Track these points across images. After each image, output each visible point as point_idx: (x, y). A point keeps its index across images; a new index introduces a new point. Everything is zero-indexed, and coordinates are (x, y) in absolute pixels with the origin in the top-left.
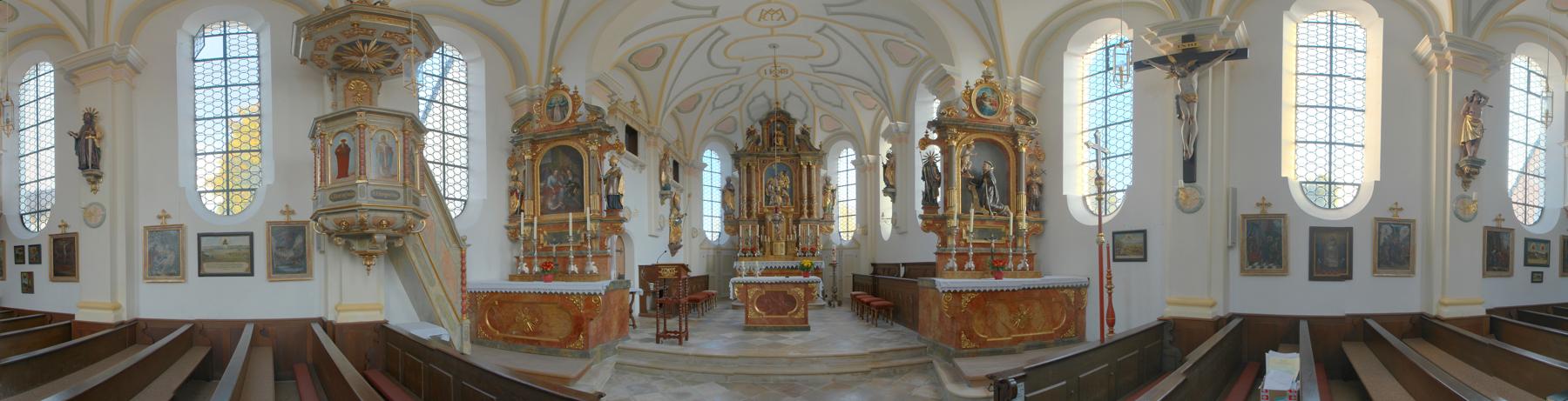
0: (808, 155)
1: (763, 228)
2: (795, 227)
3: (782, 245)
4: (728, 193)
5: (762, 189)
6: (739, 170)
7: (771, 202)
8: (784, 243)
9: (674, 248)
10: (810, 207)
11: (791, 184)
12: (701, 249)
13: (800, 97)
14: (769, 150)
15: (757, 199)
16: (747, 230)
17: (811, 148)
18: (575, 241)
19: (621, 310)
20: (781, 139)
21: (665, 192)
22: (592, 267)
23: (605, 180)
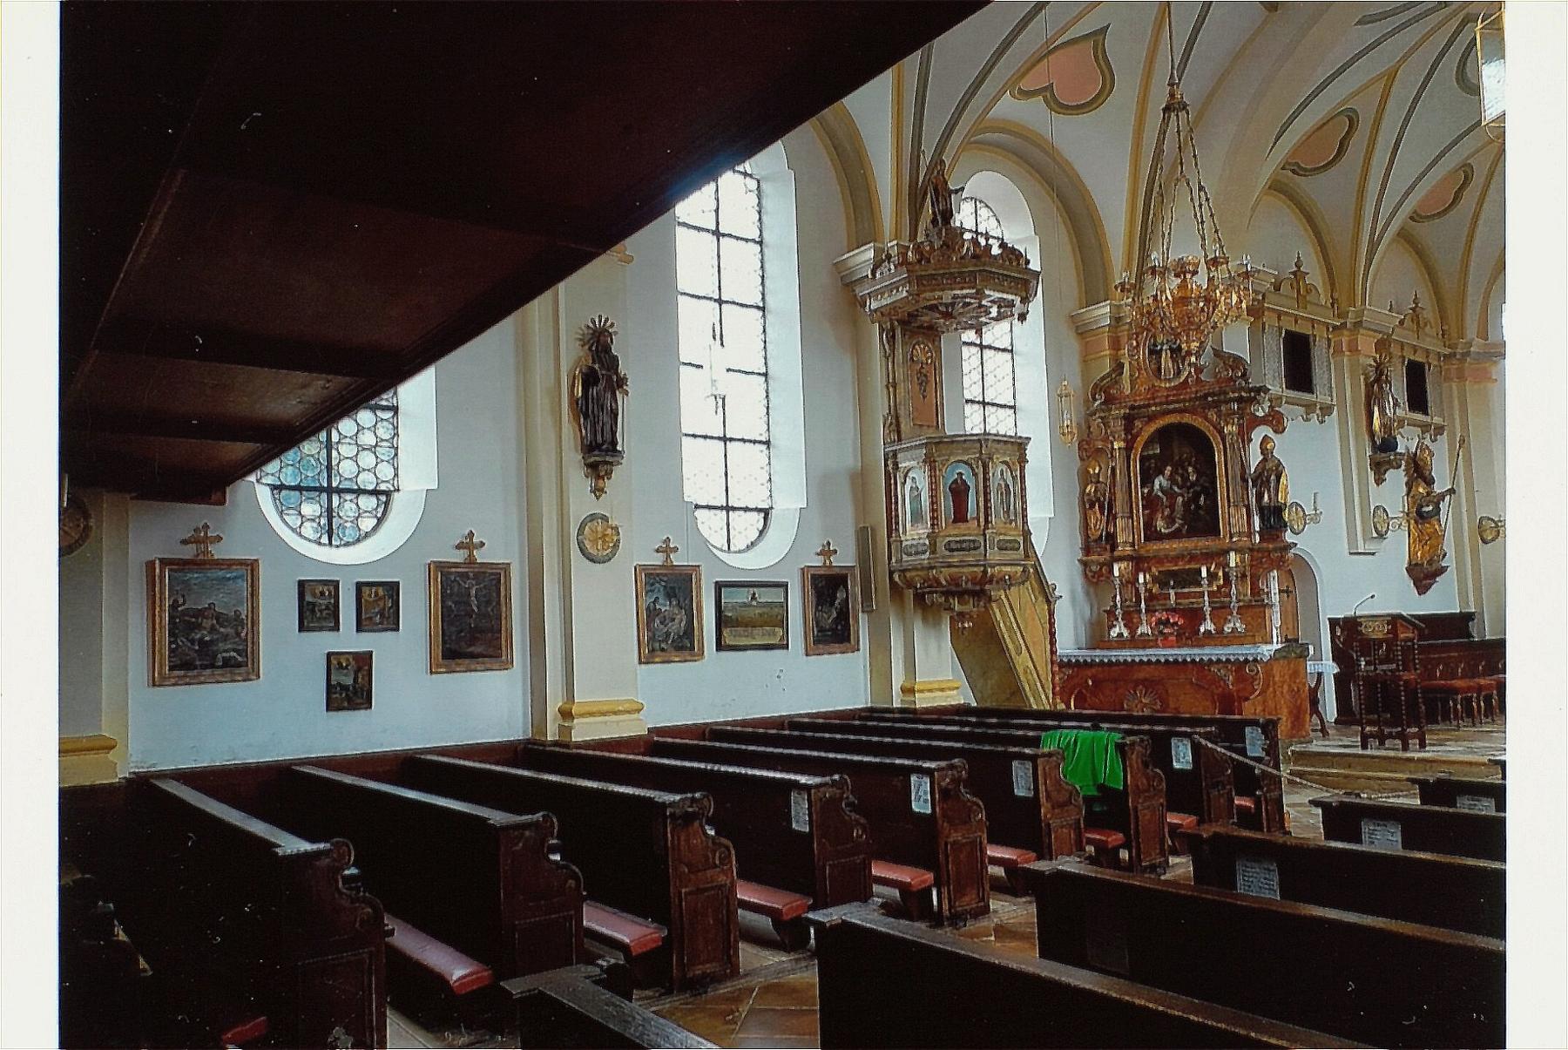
9: (1423, 575)
18: (1210, 584)
19: (1295, 694)
21: (1381, 456)
22: (1235, 624)
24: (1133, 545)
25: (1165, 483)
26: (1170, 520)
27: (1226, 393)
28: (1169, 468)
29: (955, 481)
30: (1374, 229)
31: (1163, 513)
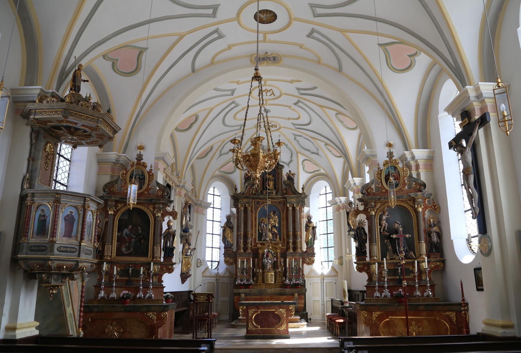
0: (293, 198)
1: (256, 260)
2: (282, 260)
4: (228, 231)
5: (256, 226)
8: (273, 273)
10: (295, 243)
11: (279, 223)
12: (203, 277)
13: (286, 145)
14: (262, 193)
15: (252, 235)
16: (243, 262)
17: (295, 192)
20: (271, 183)
23: (165, 237)
24: (111, 257)
25: (128, 232)
26: (128, 248)
27: (160, 200)
28: (130, 226)
29: (68, 216)
30: (191, 156)
31: (125, 245)
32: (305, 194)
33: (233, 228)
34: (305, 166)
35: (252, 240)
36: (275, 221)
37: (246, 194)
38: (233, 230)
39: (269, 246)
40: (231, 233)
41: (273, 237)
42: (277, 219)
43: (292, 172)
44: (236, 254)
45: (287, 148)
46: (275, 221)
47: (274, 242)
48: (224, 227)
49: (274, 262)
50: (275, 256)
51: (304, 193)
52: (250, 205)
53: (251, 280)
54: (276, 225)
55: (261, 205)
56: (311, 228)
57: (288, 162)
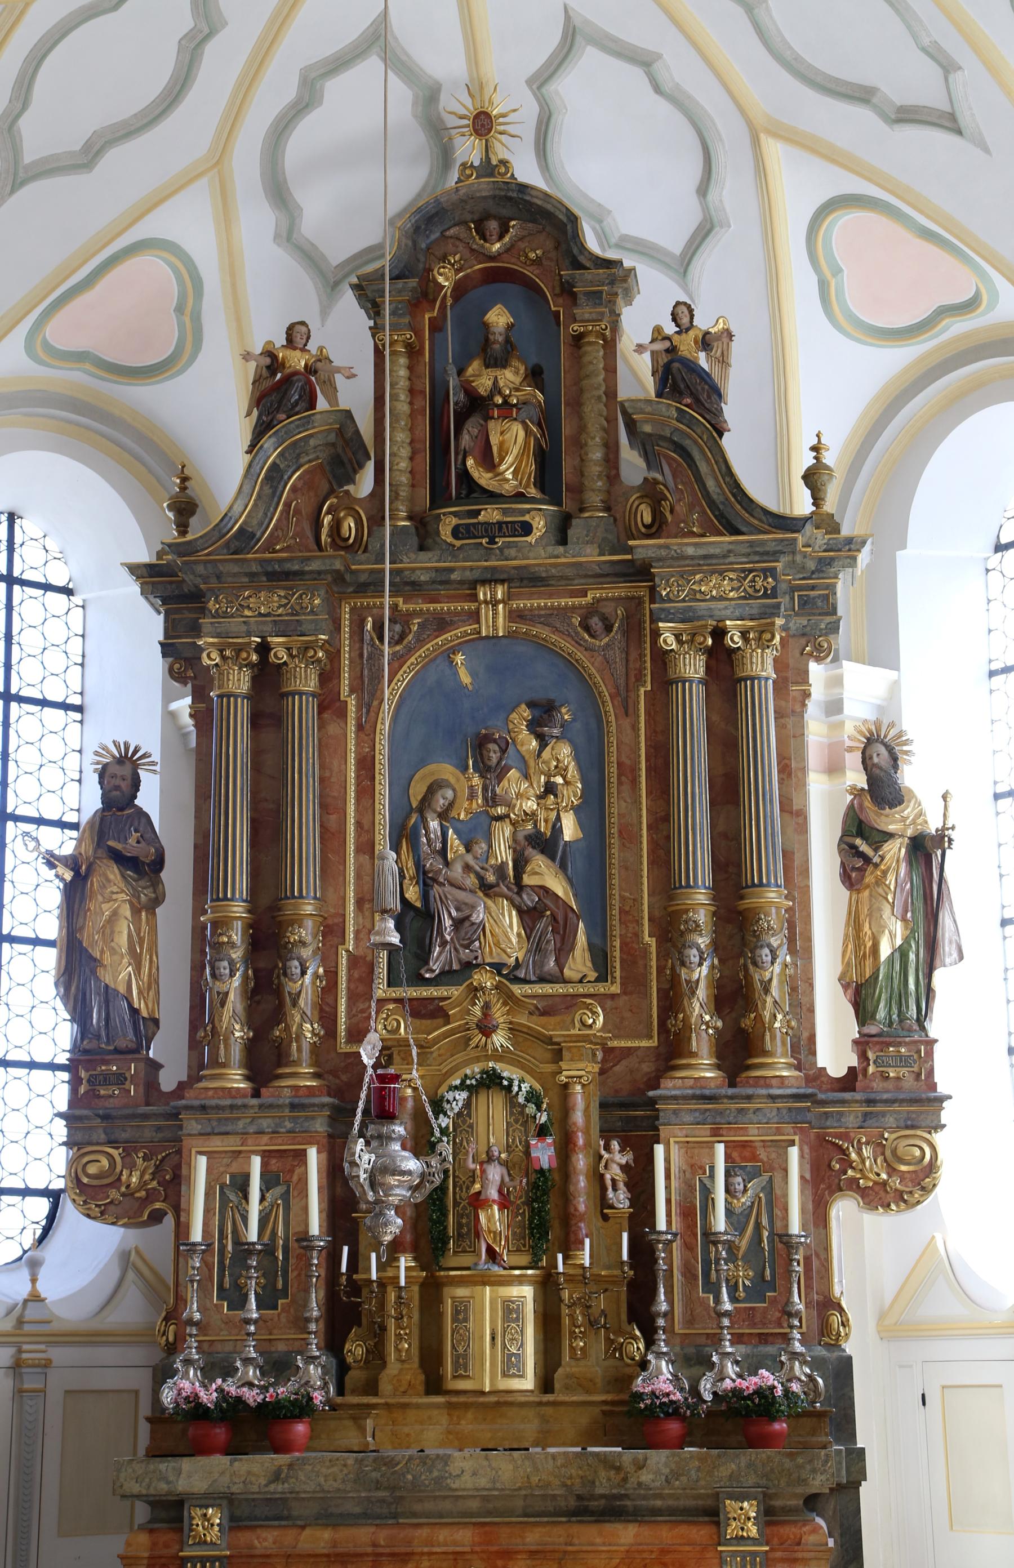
3: (510, 1311)
6: (199, 695)
7: (438, 961)
8: (527, 1292)
32: (836, 529)
33: (159, 863)
34: (837, 271)
35: (332, 975)
36: (550, 789)
37: (269, 547)
38: (156, 883)
39: (486, 1029)
40: (136, 911)
41: (537, 949)
42: (572, 771)
43: (703, 321)
44: (175, 1115)
45: (657, 89)
46: (550, 789)
47: (539, 989)
48: (73, 862)
49: (534, 1186)
50: (543, 1118)
51: (829, 523)
52: (306, 648)
53: (311, 1359)
54: (557, 830)
55: (420, 642)
56: (895, 851)
57: (676, 245)
